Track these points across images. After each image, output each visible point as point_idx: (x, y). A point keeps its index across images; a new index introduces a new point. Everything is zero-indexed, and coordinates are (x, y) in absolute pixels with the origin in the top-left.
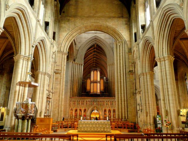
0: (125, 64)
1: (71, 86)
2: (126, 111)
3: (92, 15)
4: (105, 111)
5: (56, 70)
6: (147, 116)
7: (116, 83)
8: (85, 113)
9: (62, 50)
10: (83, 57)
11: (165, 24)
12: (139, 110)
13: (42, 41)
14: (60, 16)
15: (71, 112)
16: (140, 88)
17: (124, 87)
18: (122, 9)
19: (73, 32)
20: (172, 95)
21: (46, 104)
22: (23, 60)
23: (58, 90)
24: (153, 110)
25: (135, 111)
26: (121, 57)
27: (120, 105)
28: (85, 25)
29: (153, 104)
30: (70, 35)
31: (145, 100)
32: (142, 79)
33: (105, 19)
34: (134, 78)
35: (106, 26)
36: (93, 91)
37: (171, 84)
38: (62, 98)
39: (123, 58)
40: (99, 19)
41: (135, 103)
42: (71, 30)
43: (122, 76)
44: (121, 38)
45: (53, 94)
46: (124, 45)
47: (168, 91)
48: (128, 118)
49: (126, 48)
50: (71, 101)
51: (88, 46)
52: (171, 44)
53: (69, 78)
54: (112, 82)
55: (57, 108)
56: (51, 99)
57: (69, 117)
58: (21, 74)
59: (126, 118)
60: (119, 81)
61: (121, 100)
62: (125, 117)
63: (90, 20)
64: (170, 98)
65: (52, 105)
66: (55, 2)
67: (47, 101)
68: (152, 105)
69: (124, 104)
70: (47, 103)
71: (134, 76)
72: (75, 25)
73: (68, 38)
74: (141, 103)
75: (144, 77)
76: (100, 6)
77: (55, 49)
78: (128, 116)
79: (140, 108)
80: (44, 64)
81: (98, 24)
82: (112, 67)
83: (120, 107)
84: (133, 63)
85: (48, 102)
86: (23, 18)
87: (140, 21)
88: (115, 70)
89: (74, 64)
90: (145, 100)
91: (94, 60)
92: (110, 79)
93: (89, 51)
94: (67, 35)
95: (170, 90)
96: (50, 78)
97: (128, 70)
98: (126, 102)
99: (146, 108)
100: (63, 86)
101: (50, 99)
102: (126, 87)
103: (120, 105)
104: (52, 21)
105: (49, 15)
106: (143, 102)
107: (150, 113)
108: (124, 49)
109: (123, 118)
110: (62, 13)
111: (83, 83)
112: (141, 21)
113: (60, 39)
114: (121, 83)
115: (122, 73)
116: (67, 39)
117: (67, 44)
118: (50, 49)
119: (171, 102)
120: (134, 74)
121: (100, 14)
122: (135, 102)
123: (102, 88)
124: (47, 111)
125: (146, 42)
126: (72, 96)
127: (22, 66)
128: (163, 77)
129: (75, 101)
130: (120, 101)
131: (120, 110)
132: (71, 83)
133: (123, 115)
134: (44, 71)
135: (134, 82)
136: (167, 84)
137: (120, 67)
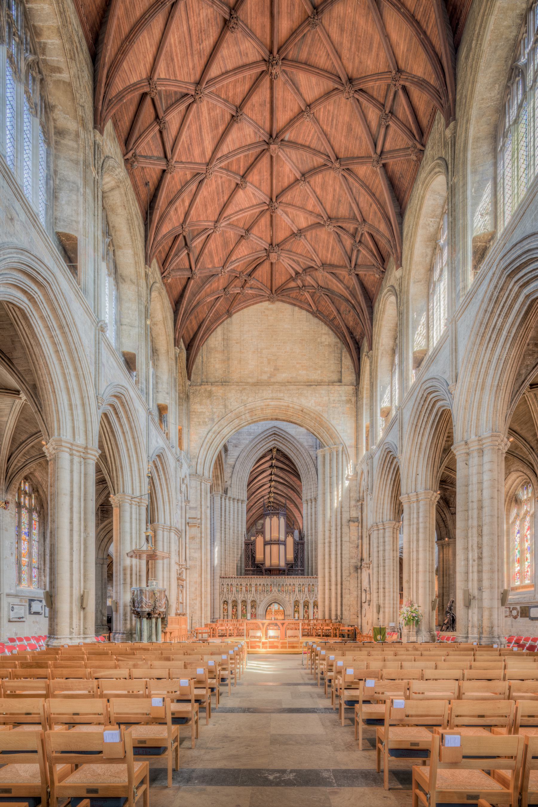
3: (265, 377)
6: (378, 612)
7: (320, 546)
8: (254, 610)
9: (200, 471)
10: (246, 483)
13: (158, 456)
20: (425, 572)
21: (176, 591)
22: (131, 504)
23: (198, 563)
24: (392, 602)
25: (357, 604)
27: (327, 591)
28: (250, 407)
29: (392, 590)
31: (378, 582)
37: (425, 550)
38: (206, 579)
40: (283, 388)
42: (216, 420)
45: (188, 571)
47: (418, 565)
51: (259, 452)
52: (436, 464)
54: (312, 542)
55: (199, 599)
56: (185, 582)
62: (336, 615)
64: (421, 578)
65: (188, 593)
67: (178, 585)
68: (389, 592)
69: (336, 589)
70: (178, 589)
76: (285, 352)
78: (342, 614)
79: (368, 598)
81: (281, 404)
82: (313, 506)
83: (327, 596)
85: (181, 588)
86: (122, 414)
90: (378, 582)
93: (258, 467)
95: (421, 562)
101: (183, 580)
107: (384, 607)
109: (333, 617)
111: (247, 544)
118: (176, 471)
119: (421, 584)
124: (181, 605)
125: (388, 453)
133: (333, 613)
134: (168, 523)
136: (417, 551)
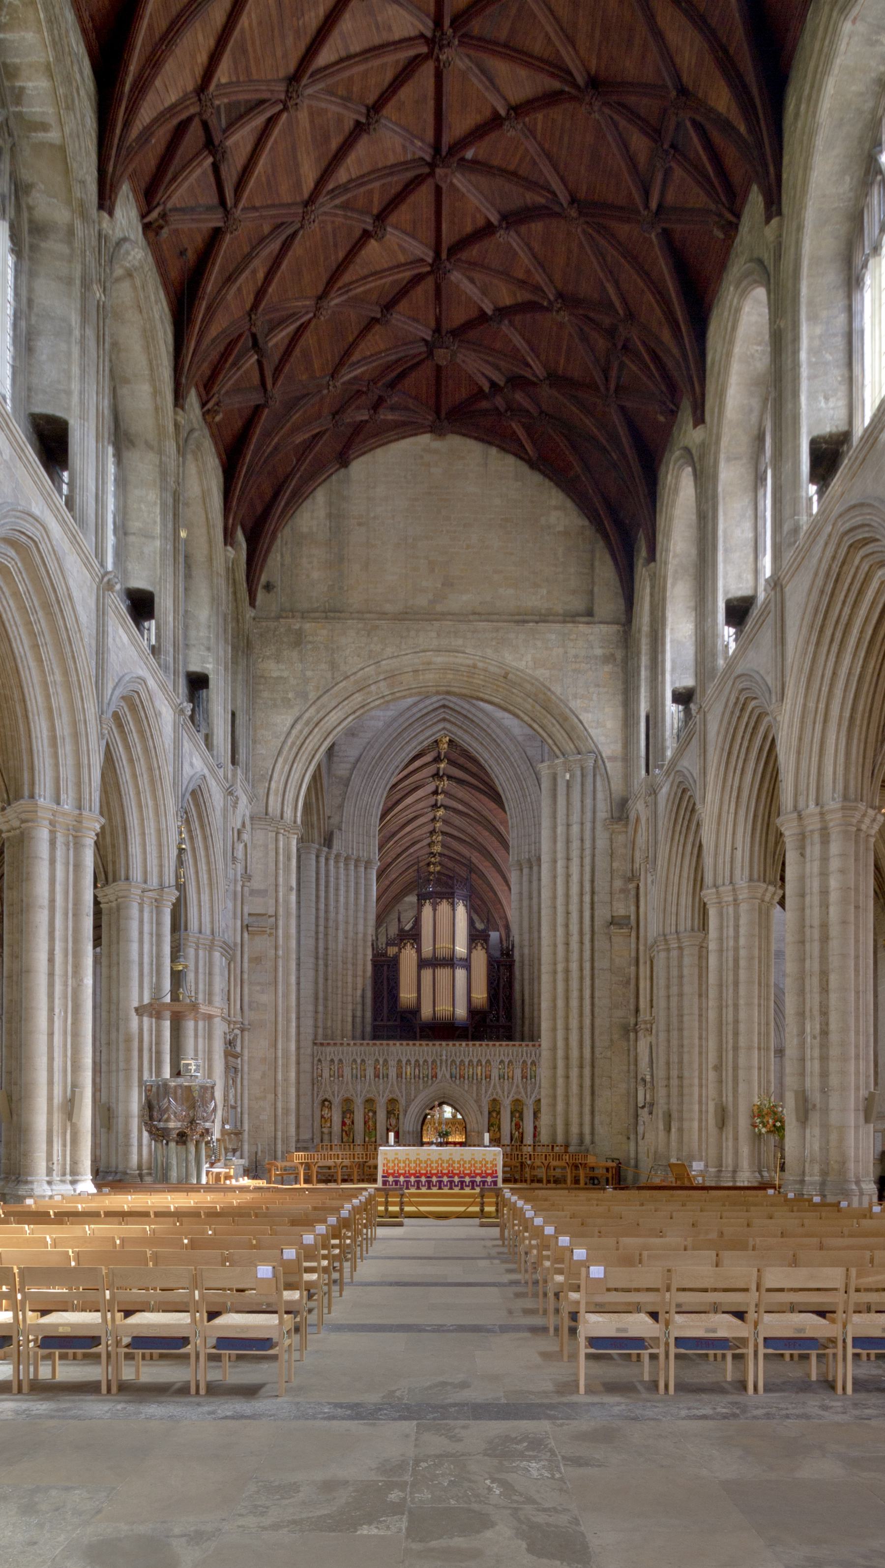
0: (592, 881)
1: (316, 983)
2: (587, 1109)
3: (422, 601)
4: (494, 1110)
5: (250, 915)
7: (545, 978)
11: (745, 744)
12: (643, 1107)
14: (250, 613)
15: (322, 1117)
16: (652, 1007)
17: (581, 998)
18: (592, 561)
19: (323, 706)
26: (575, 845)
27: (560, 1081)
30: (312, 725)
32: (661, 960)
33: (497, 630)
34: (633, 954)
35: (497, 670)
36: (431, 1010)
38: (286, 1051)
39: (582, 849)
41: (632, 1074)
42: (312, 696)
43: (574, 945)
44: (577, 742)
45: (246, 1033)
46: (589, 780)
48: (593, 1142)
49: (600, 795)
50: (319, 1060)
53: (309, 943)
55: (271, 1097)
57: (312, 1139)
58: (141, 964)
59: (587, 1138)
60: (560, 967)
61: (567, 1058)
62: (581, 1135)
63: (412, 633)
65: (246, 1083)
66: (229, 548)
69: (581, 1076)
71: (633, 946)
72: (333, 666)
73: (298, 743)
74: (652, 1076)
75: (668, 958)
77: (244, 807)
78: (592, 1133)
80: (205, 897)
83: (560, 1092)
84: (630, 880)
87: (668, 666)
88: (543, 912)
89: (327, 859)
91: (434, 819)
92: (526, 943)
94: (293, 726)
96: (231, 960)
97: (603, 914)
98: (587, 1071)
99: (669, 1096)
100: (286, 996)
102: (592, 997)
103: (560, 1081)
104: (221, 668)
105: (203, 633)
106: (660, 1073)
108: (589, 801)
109: (574, 1140)
110: (260, 595)
112: (673, 669)
113: (262, 750)
114: (567, 980)
115: (574, 929)
116: (295, 750)
117: (295, 776)
120: (634, 934)
121: (465, 598)
122: (632, 1067)
123: (480, 995)
126: (325, 1036)
127: (141, 933)
128: (724, 973)
129: (340, 1061)
130: (560, 1064)
131: (560, 1107)
132: (317, 965)
135: (633, 976)
137: (567, 896)
